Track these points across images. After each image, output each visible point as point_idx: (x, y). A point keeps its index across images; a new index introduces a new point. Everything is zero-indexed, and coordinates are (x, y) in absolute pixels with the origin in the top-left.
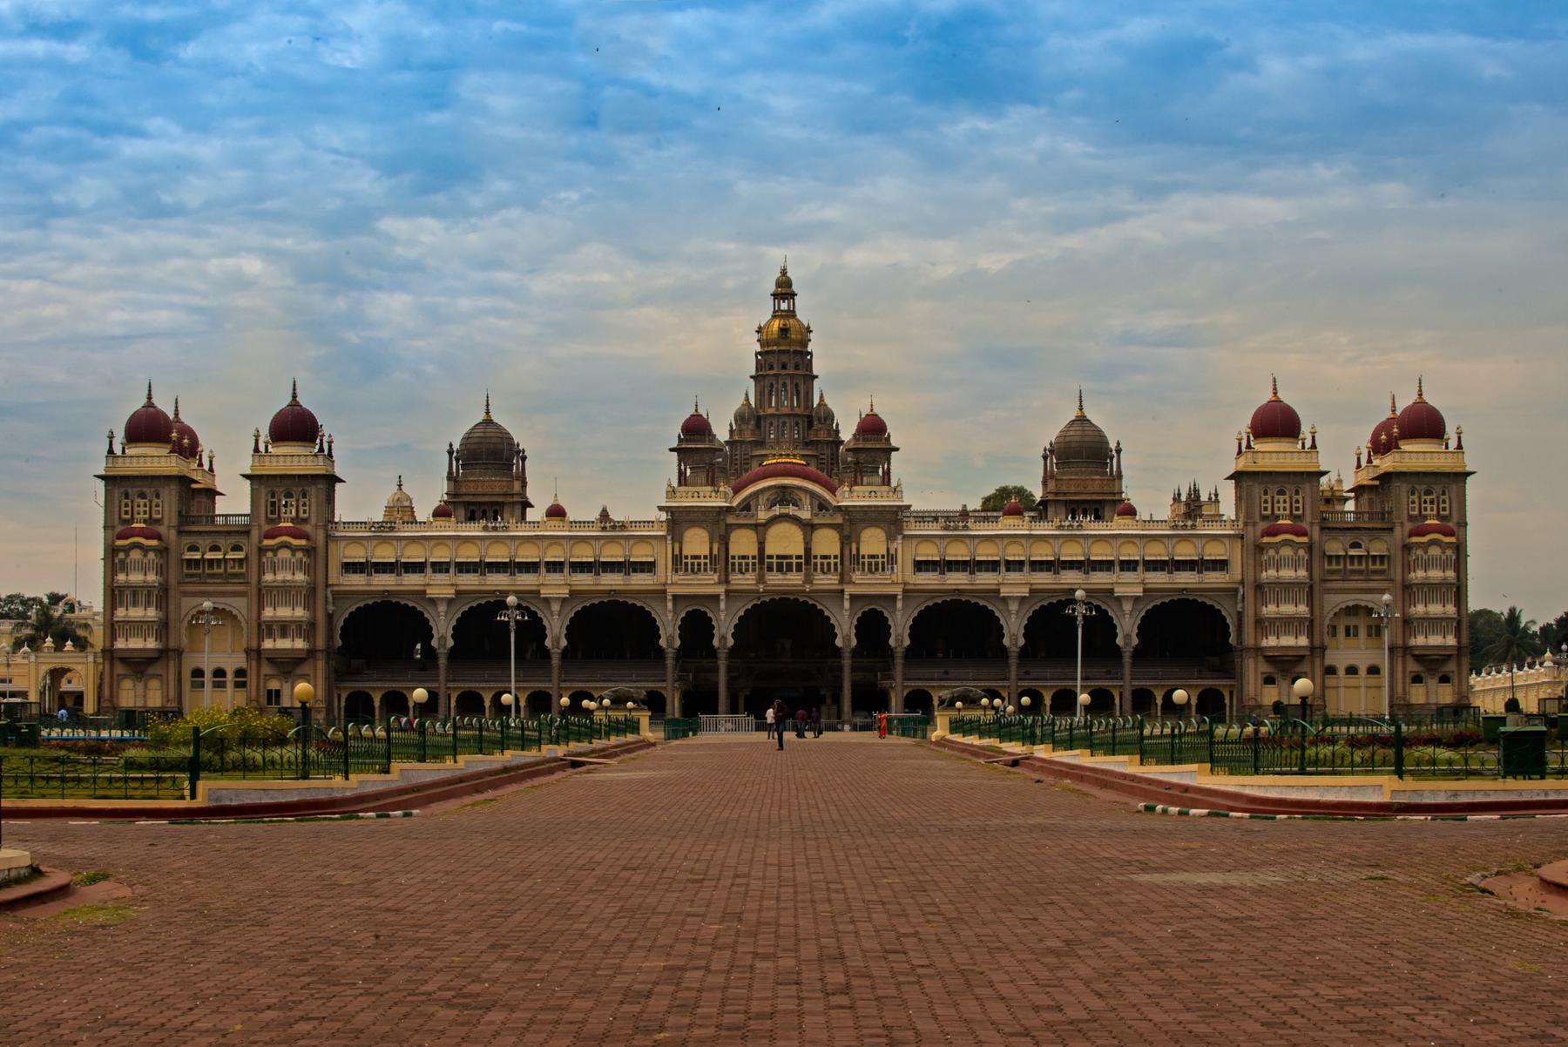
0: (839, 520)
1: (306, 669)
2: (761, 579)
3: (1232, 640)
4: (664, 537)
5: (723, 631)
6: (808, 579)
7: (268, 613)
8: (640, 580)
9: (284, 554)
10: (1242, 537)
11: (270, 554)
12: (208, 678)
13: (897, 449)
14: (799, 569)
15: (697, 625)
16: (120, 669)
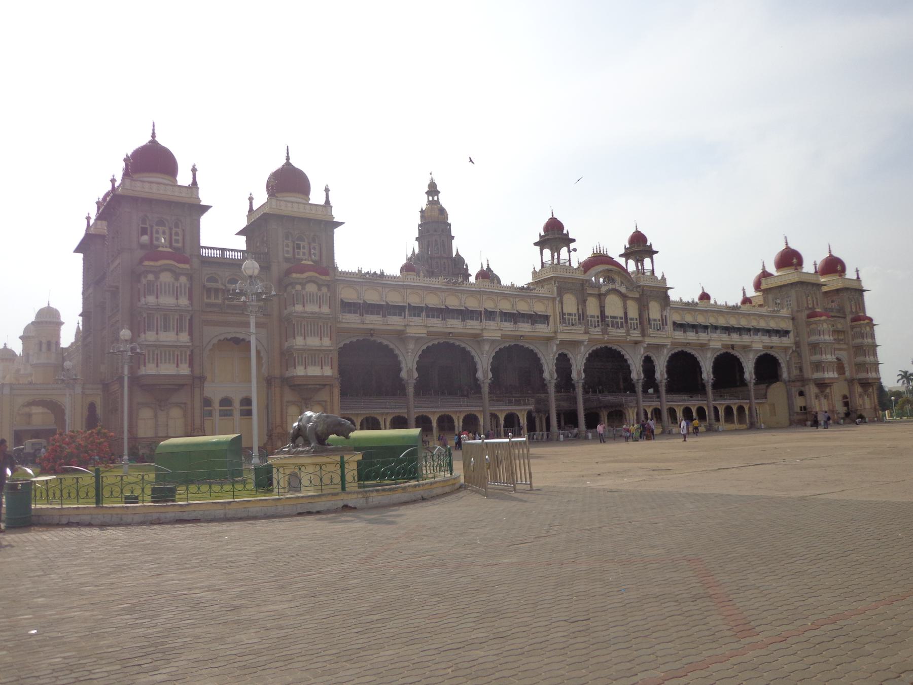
0: (637, 296)
1: (324, 395)
2: (604, 332)
3: (785, 375)
4: (554, 299)
5: (579, 367)
6: (628, 334)
7: (299, 341)
8: (541, 329)
9: (311, 288)
10: (793, 319)
11: (298, 287)
12: (216, 405)
13: (656, 252)
14: (622, 327)
15: (563, 363)
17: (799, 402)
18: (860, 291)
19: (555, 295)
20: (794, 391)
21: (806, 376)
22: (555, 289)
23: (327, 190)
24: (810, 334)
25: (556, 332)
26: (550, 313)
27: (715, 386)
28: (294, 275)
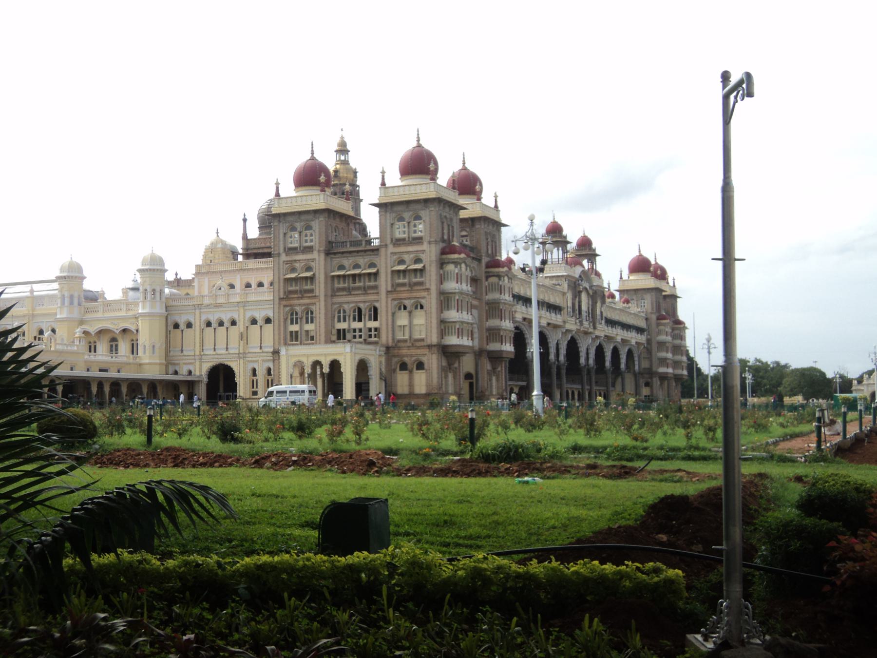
0: (591, 292)
3: (637, 368)
4: (564, 294)
10: (647, 319)
16: (444, 363)
17: (645, 391)
18: (674, 297)
19: (566, 290)
20: (642, 382)
21: (654, 369)
22: (566, 286)
23: (496, 197)
24: (659, 333)
25: (564, 322)
26: (561, 305)
27: (612, 373)
28: (501, 270)
